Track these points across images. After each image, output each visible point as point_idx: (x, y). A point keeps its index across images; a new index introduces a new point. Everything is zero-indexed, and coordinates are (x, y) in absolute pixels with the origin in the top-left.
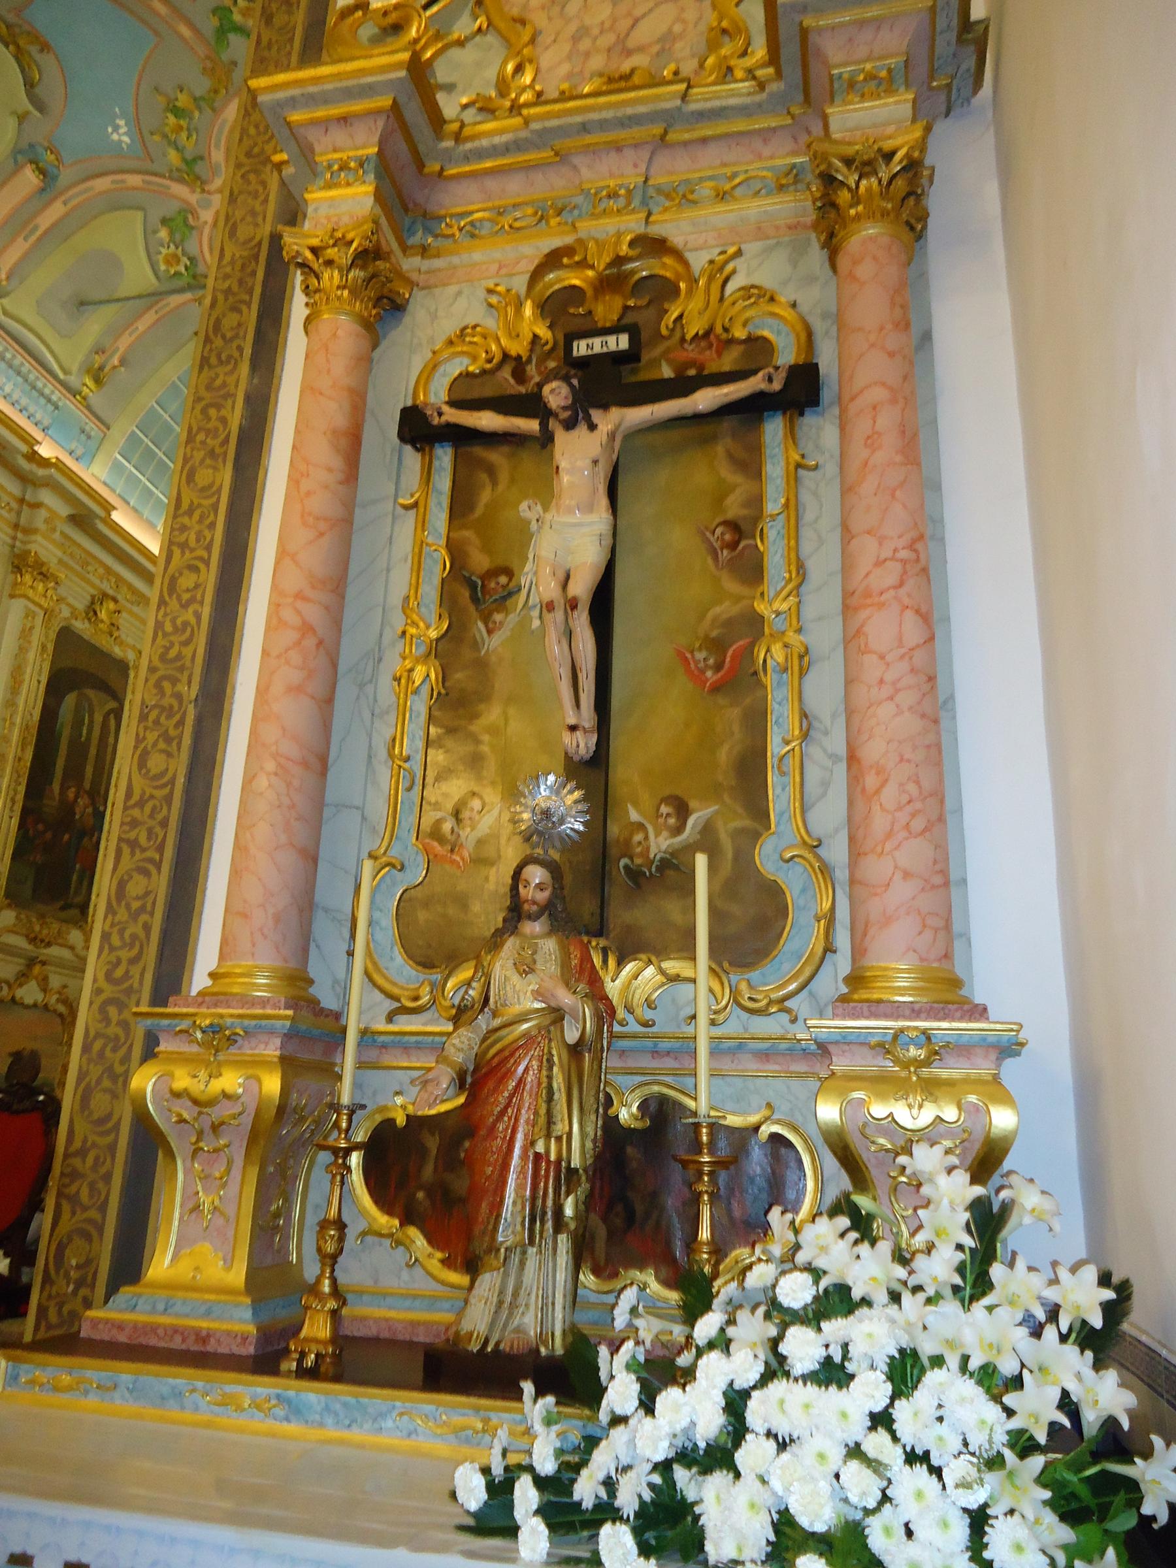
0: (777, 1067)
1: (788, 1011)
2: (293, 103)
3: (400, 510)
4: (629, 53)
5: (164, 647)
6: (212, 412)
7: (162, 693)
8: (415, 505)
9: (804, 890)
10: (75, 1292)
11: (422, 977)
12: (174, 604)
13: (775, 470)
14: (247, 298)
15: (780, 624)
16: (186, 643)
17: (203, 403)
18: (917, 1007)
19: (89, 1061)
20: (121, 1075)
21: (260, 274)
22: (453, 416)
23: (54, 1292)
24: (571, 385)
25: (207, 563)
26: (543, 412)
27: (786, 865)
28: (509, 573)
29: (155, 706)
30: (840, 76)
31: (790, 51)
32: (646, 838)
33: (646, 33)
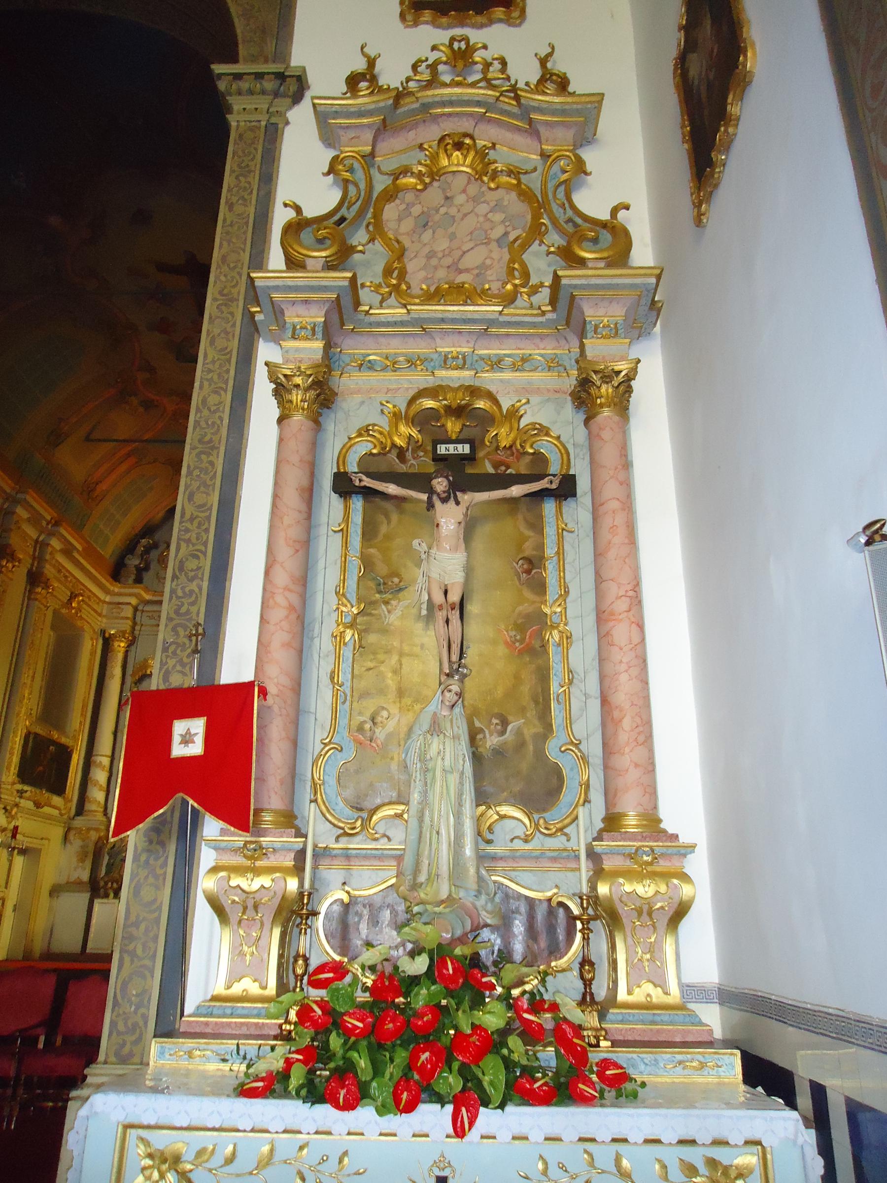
0: (560, 866)
1: (566, 834)
2: (277, 288)
3: (331, 533)
4: (461, 272)
5: (178, 605)
6: (203, 457)
7: (177, 634)
8: (342, 530)
9: (572, 769)
10: (135, 1012)
11: (356, 815)
12: (183, 578)
13: (550, 531)
14: (224, 386)
15: (555, 619)
16: (193, 604)
17: (197, 450)
18: (644, 835)
19: (139, 866)
20: (161, 875)
21: (232, 373)
22: (367, 482)
23: (121, 1012)
24: (449, 480)
25: (205, 554)
26: (431, 491)
27: (562, 754)
28: (398, 575)
29: (172, 643)
30: (590, 322)
31: (563, 303)
32: (485, 737)
33: (471, 260)
